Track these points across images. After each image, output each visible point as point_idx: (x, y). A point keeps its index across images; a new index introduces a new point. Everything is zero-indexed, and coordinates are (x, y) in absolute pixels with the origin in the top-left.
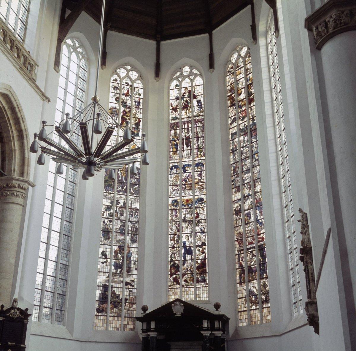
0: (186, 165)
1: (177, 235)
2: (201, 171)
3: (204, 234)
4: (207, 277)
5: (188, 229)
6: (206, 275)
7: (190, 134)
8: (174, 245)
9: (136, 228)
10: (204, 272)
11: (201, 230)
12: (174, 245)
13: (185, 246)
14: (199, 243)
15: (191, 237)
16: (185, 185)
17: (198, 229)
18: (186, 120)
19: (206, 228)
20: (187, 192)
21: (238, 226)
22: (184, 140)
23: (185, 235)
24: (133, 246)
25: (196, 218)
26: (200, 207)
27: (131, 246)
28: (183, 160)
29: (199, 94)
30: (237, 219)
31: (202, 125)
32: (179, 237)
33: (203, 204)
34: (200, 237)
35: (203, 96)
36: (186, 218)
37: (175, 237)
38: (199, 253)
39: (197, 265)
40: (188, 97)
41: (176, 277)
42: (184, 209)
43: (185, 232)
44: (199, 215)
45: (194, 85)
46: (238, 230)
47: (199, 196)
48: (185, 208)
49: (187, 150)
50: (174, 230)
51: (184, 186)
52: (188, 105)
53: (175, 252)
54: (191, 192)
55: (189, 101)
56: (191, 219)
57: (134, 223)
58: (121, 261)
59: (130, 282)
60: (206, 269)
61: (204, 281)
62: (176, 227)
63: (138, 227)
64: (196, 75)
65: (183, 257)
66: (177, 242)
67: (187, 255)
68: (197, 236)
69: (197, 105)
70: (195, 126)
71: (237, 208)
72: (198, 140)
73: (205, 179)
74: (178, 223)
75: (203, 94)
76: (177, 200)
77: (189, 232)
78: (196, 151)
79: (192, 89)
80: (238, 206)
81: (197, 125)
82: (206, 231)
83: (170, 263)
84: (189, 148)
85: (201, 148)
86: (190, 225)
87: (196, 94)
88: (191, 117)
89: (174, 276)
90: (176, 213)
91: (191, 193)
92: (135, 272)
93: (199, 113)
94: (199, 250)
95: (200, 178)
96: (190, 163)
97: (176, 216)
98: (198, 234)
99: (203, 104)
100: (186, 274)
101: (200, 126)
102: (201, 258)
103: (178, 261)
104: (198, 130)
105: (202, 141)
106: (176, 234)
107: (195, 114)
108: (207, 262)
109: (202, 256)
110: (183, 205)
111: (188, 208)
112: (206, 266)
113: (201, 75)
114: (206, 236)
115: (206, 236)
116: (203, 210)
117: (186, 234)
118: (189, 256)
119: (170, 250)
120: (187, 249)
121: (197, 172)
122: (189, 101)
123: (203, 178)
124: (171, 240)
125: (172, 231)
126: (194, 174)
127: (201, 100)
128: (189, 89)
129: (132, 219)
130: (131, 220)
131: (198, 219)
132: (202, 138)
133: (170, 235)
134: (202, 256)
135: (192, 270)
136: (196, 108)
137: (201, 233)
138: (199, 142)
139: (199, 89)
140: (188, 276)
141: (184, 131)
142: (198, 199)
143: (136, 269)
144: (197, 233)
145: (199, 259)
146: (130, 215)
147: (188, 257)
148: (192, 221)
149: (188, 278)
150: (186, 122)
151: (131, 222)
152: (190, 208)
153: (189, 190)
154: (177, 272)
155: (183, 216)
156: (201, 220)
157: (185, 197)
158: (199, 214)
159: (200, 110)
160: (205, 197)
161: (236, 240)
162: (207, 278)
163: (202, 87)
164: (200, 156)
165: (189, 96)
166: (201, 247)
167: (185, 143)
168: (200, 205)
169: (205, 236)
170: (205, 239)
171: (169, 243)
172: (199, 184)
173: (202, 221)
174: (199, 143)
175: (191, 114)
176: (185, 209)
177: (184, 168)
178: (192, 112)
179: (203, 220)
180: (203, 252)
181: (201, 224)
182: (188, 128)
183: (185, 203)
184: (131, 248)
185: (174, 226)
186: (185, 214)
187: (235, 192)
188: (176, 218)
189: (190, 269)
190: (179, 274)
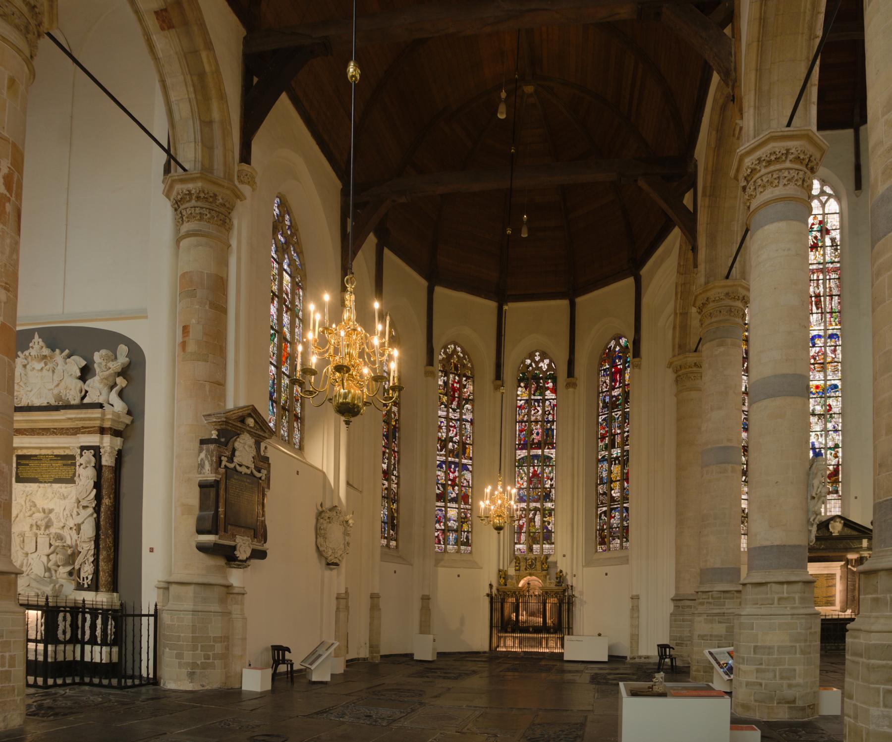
0: (815, 336)
2: (835, 346)
7: (821, 290)
10: (837, 481)
11: (834, 427)
13: (814, 449)
14: (830, 444)
15: (821, 435)
16: (813, 364)
17: (830, 426)
18: (815, 267)
20: (817, 374)
22: (813, 299)
23: (814, 433)
26: (833, 397)
28: (811, 328)
29: (834, 228)
31: (837, 277)
33: (837, 393)
35: (838, 231)
40: (818, 231)
42: (812, 398)
43: (814, 430)
45: (826, 212)
48: (814, 396)
49: (817, 313)
51: (812, 366)
52: (818, 244)
54: (821, 375)
55: (819, 237)
58: (745, 466)
61: (837, 492)
64: (830, 196)
69: (831, 244)
70: (828, 277)
72: (832, 299)
73: (840, 357)
75: (838, 227)
78: (828, 316)
79: (824, 218)
81: (830, 276)
82: (840, 428)
84: (820, 311)
85: (835, 312)
86: (820, 421)
87: (829, 226)
88: (822, 264)
91: (822, 377)
93: (834, 259)
94: (831, 454)
95: (834, 356)
96: (820, 334)
98: (830, 432)
99: (839, 243)
101: (834, 279)
102: (833, 463)
104: (833, 285)
105: (836, 301)
107: (828, 259)
109: (834, 462)
112: (839, 474)
113: (838, 198)
114: (840, 436)
116: (837, 400)
117: (815, 431)
120: (816, 452)
121: (830, 346)
122: (819, 237)
123: (837, 356)
126: (825, 349)
127: (835, 239)
128: (820, 218)
131: (831, 412)
132: (837, 297)
136: (829, 250)
137: (834, 431)
138: (833, 303)
139: (833, 220)
141: (812, 284)
142: (830, 385)
144: (828, 431)
145: (831, 465)
148: (823, 415)
150: (815, 271)
152: (821, 397)
153: (819, 371)
156: (834, 414)
157: (813, 382)
159: (834, 254)
160: (840, 383)
162: (840, 489)
163: (837, 217)
164: (834, 324)
165: (820, 231)
166: (834, 450)
167: (814, 303)
168: (833, 394)
172: (833, 364)
174: (833, 305)
175: (822, 258)
176: (815, 398)
177: (813, 338)
178: (824, 255)
179: (837, 414)
180: (836, 456)
182: (818, 280)
183: (813, 390)
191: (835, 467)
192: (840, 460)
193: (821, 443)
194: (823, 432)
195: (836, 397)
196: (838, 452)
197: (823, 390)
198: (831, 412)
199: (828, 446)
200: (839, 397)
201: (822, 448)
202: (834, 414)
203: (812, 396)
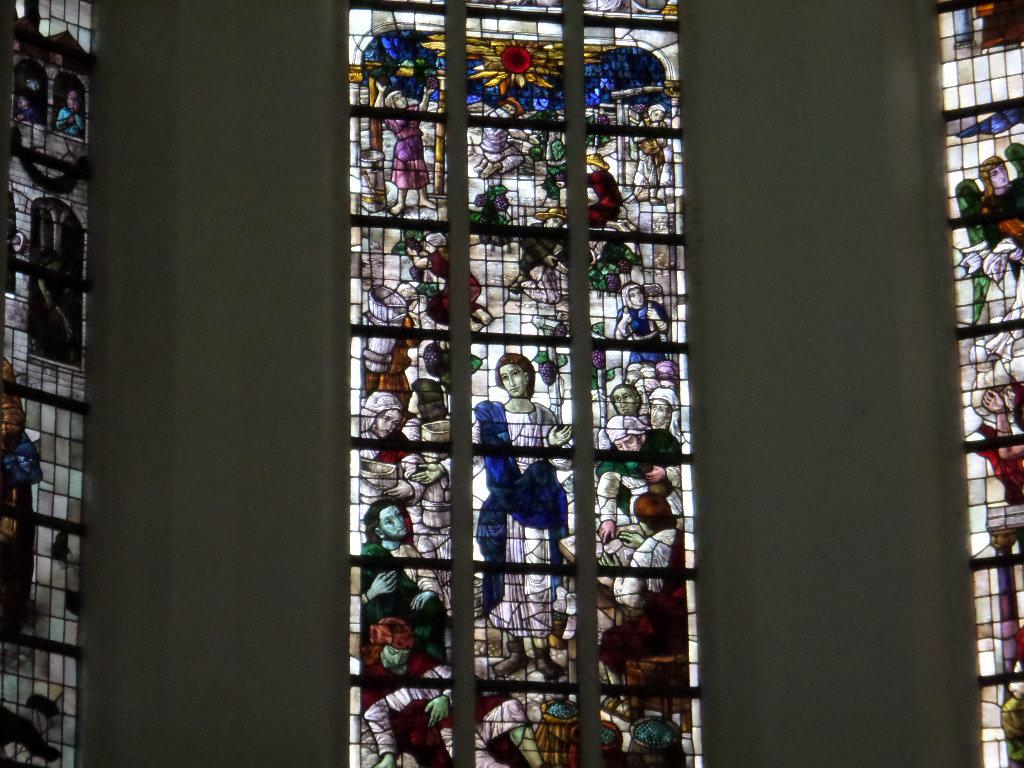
1: (426, 343)
3: (663, 368)
4: (696, 731)
5: (528, 309)
6: (686, 714)
8: (400, 424)
9: (72, 230)
10: (670, 688)
11: (640, 324)
12: (400, 424)
13: (497, 449)
14: (615, 431)
15: (552, 373)
19: (682, 311)
21: (993, 330)
23: (496, 351)
24: (49, 388)
25: (594, 224)
26: (626, 130)
27: (35, 384)
30: (990, 267)
32: (439, 363)
33: (656, 110)
34: (632, 387)
36: (506, 204)
37: (407, 362)
38: (622, 519)
39: (603, 621)
41: (417, 708)
42: (483, 123)
43: (497, 328)
44: (618, 201)
46: (993, 358)
47: (620, 32)
50: (396, 300)
53: (403, 488)
56: (551, 223)
57: (54, 174)
59: (23, 711)
60: (687, 663)
62: (418, 274)
63: (82, 217)
65: (483, 541)
66: (422, 402)
67: (514, 527)
68: (606, 379)
71: (987, 180)
74: (433, 241)
76: (425, 37)
77: (530, 330)
80: (996, 163)
82: (679, 334)
83: (366, 584)
86: (537, 273)
89: (401, 698)
90: (418, 153)
92: (61, 628)
94: (622, 496)
97: (417, 178)
98: (612, 355)
100: (500, 689)
102: (640, 559)
103: (435, 564)
106: (418, 335)
108: (691, 605)
110: (476, 87)
111: (521, 125)
114: (684, 386)
115: (684, 386)
116: (658, 161)
117: (506, 339)
118: (531, 533)
119: (364, 465)
124: (370, 386)
125: (379, 300)
129: (33, 135)
130: (26, 142)
131: (611, 226)
133: (366, 332)
134: (648, 544)
135: (558, 656)
140: (524, 708)
143: (73, 602)
145: (624, 571)
146: (23, 103)
147: (528, 543)
148: (557, 235)
149: (527, 723)
151: (29, 158)
152: (544, 125)
154: (434, 662)
155: (477, 187)
157: (490, 24)
158: (626, 194)
160: (673, 50)
161: (979, 437)
166: (639, 474)
168: (623, 114)
169: (675, 379)
170: (670, 408)
171: (355, 409)
173: (647, 249)
176: (497, 123)
179: (655, 239)
180: (657, 515)
181: (636, 275)
183: (490, 75)
184: (30, 406)
185: (393, 261)
186: (498, 172)
187: (966, 40)
188: (412, 195)
189: (544, 653)
190: (440, 684)
191: (652, 584)
192: (689, 542)
193: (546, 419)
194: (563, 350)
195: (650, 133)
196: (669, 487)
197: (558, 82)
198: (611, 226)
199: (603, 444)
200: (669, 133)
201: (556, 451)
202: (640, 236)
203: (477, 107)
